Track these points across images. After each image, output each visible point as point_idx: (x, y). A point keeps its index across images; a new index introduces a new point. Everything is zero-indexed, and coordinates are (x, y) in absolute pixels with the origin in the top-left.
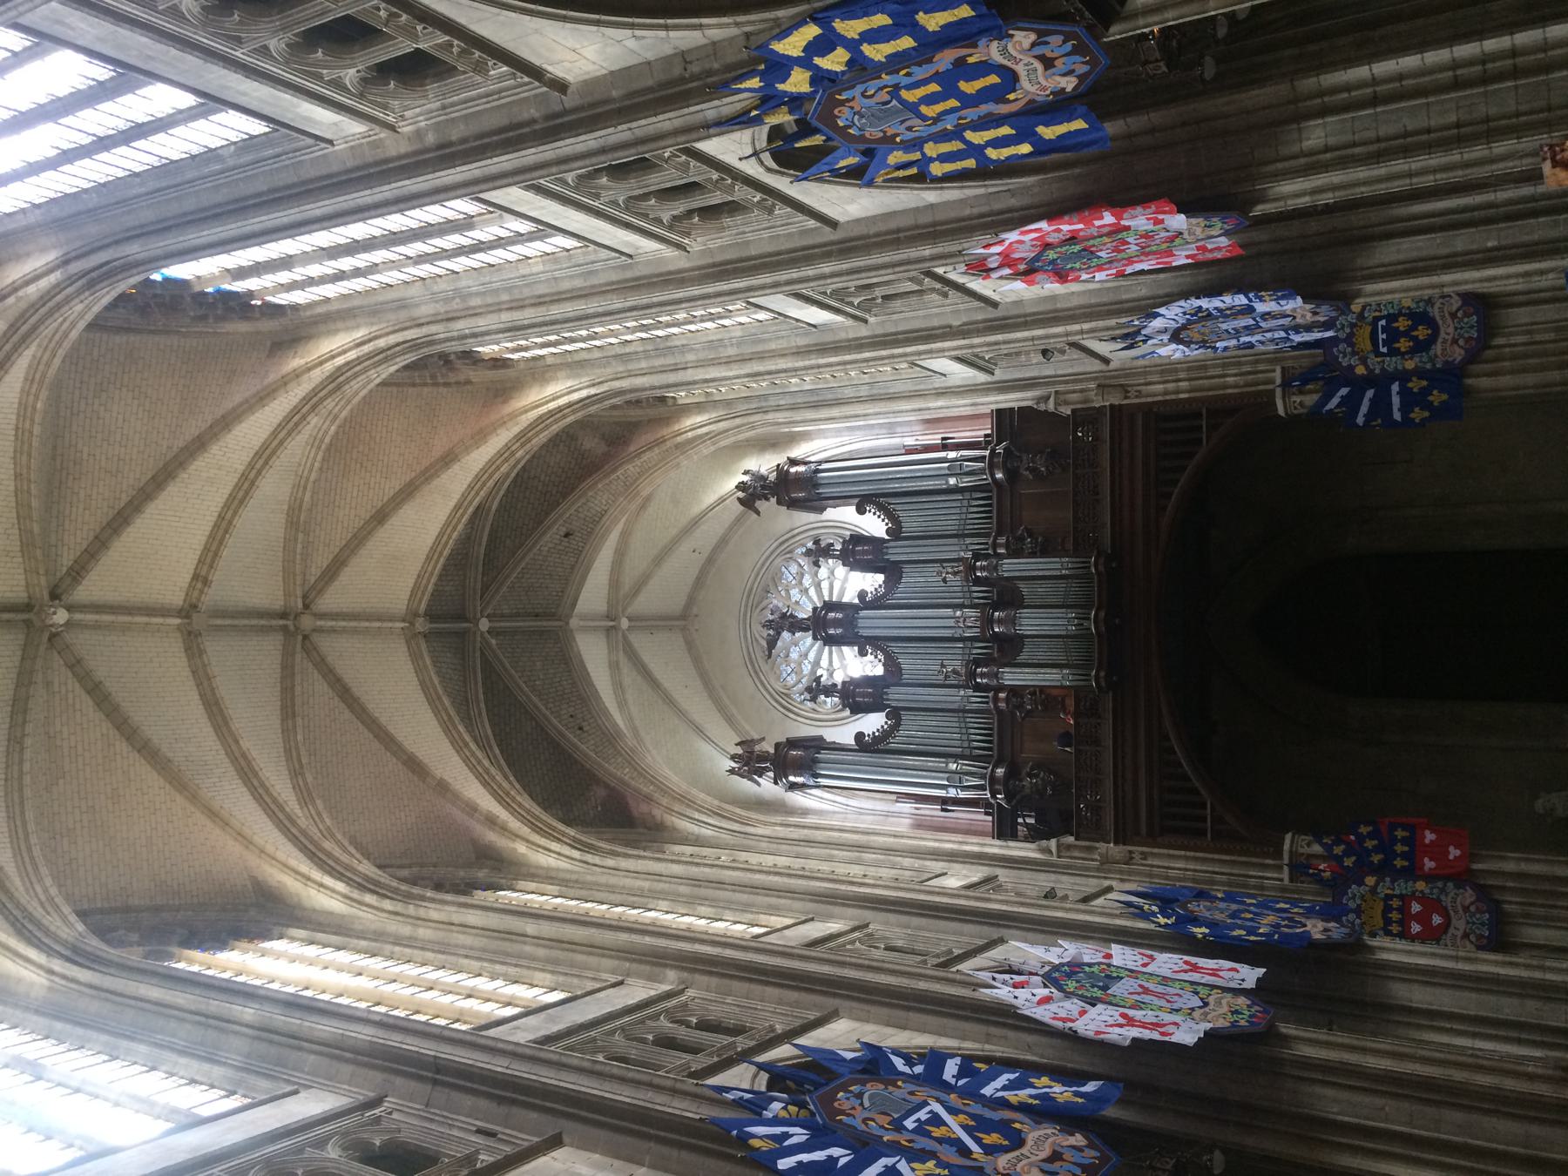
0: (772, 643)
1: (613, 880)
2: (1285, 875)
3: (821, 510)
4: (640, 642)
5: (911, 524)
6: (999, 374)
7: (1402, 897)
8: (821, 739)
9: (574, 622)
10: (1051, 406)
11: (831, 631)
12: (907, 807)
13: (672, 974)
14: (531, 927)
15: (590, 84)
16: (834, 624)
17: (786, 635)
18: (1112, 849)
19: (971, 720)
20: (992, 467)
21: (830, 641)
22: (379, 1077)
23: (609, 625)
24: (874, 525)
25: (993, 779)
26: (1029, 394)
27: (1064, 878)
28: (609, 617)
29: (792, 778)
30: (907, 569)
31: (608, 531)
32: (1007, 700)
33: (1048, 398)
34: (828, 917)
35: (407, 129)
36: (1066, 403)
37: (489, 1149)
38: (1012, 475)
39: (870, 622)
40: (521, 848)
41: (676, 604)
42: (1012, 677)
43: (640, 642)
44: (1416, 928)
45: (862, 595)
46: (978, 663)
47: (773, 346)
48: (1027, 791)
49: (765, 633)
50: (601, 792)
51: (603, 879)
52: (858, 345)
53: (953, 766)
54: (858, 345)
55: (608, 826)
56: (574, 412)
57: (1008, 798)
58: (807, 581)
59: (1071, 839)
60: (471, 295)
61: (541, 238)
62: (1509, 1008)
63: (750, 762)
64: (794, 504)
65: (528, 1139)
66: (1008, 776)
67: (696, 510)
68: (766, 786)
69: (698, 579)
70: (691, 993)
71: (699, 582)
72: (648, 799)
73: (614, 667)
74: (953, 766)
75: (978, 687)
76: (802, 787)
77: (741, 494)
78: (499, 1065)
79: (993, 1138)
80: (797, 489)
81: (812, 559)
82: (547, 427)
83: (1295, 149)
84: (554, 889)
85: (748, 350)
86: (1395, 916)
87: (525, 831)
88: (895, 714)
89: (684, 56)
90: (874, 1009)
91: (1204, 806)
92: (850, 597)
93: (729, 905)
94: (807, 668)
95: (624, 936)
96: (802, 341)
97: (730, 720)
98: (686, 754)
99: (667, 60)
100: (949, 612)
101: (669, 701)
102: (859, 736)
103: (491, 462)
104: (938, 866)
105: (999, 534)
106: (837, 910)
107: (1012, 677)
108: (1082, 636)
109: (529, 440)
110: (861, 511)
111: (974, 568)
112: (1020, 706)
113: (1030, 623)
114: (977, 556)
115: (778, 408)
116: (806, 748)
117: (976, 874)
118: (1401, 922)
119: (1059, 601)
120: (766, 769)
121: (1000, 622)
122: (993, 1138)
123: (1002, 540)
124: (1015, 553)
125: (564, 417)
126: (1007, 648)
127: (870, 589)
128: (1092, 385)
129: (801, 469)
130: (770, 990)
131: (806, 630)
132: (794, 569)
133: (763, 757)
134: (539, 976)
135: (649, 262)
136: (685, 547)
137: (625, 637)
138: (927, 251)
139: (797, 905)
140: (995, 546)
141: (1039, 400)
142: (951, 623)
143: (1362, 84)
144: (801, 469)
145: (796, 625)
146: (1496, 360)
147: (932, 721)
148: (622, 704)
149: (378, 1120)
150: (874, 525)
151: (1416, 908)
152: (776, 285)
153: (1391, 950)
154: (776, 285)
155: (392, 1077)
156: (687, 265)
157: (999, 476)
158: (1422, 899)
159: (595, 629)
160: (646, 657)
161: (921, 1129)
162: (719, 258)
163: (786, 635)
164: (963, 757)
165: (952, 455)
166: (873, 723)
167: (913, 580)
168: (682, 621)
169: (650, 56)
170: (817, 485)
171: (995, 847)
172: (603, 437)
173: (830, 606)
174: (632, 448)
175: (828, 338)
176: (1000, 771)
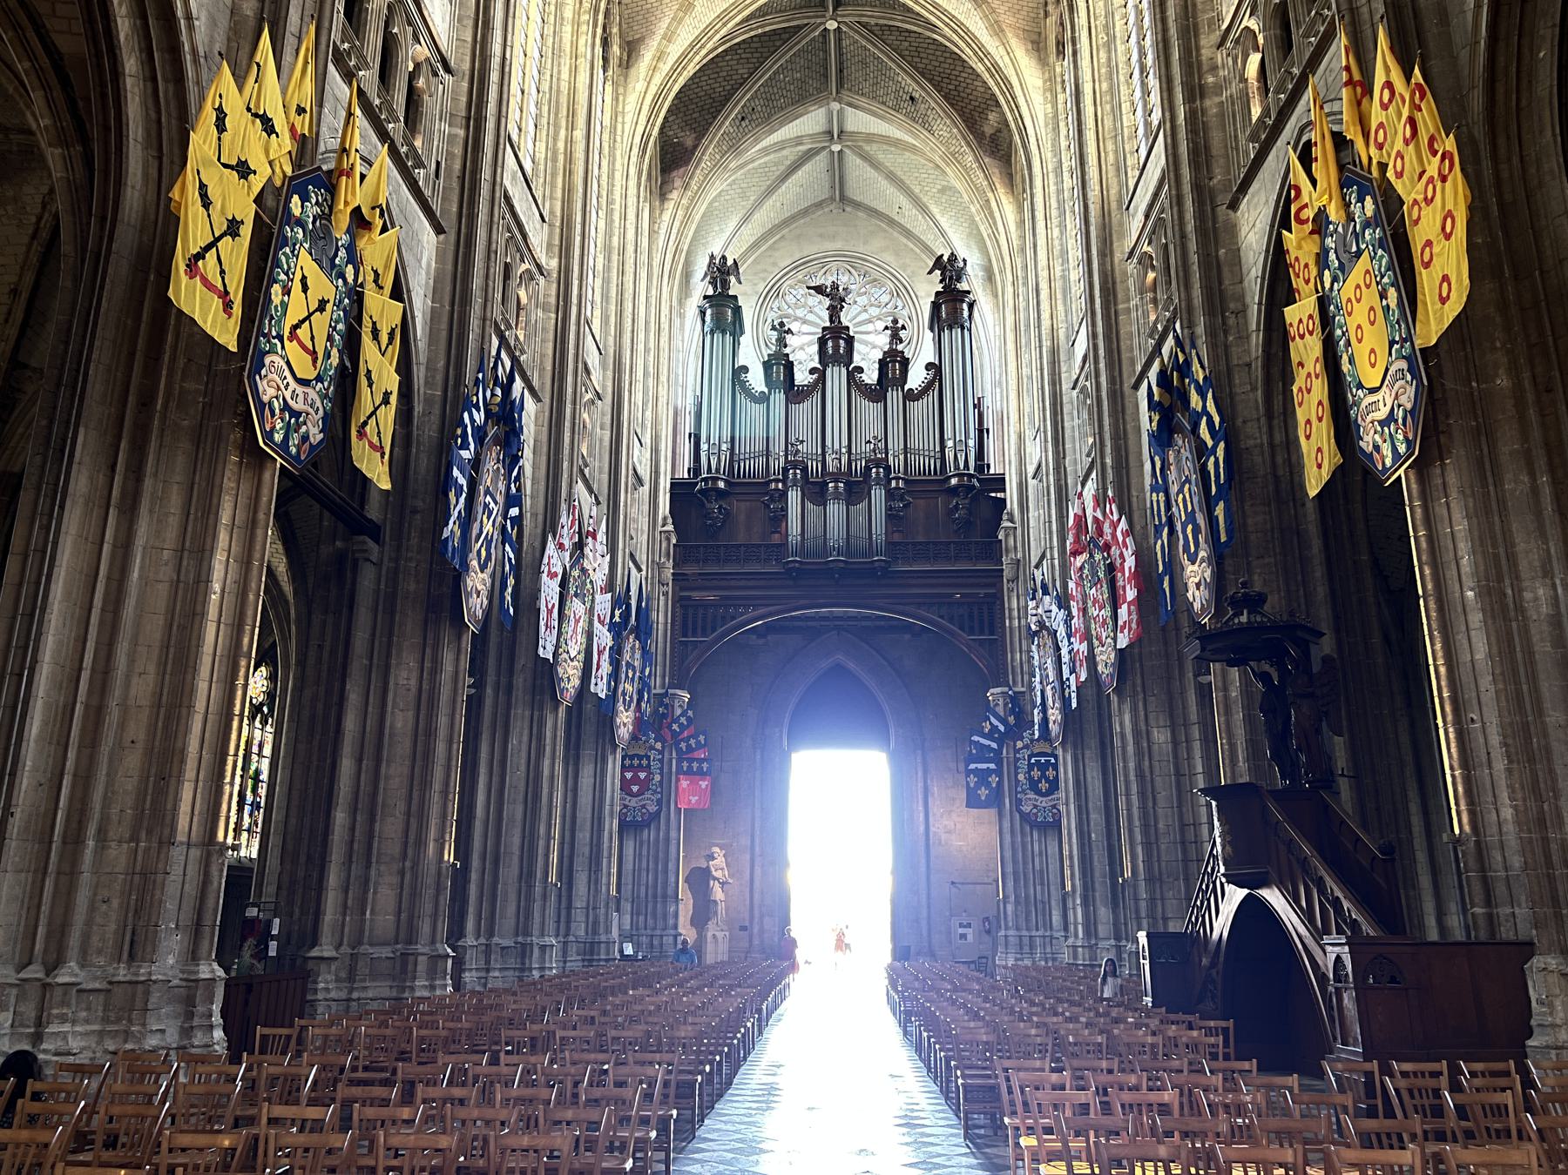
0: (819, 290)
1: (618, 175)
2: (658, 691)
3: (931, 329)
4: (820, 162)
5: (917, 408)
6: (1032, 483)
7: (649, 766)
8: (742, 333)
9: (835, 106)
10: (1006, 524)
11: (830, 344)
12: (690, 400)
13: (554, 263)
14: (579, 134)
15: (1232, 230)
16: (836, 342)
17: (827, 302)
19: (762, 461)
20: (960, 476)
21: (822, 342)
22: (466, 66)
23: (835, 133)
25: (716, 479)
26: (1015, 506)
27: (645, 537)
28: (841, 132)
29: (709, 312)
30: (880, 405)
31: (916, 137)
32: (777, 489)
33: (1012, 521)
34: (604, 366)
35: (1219, 57)
36: (1007, 536)
37: (427, 176)
38: (954, 491)
39: (836, 378)
40: (640, 86)
41: (853, 192)
42: (794, 497)
43: (820, 162)
44: (629, 775)
45: (860, 370)
46: (805, 470)
47: (1060, 307)
48: (708, 505)
49: (829, 283)
50: (689, 142)
51: (618, 166)
52: (1055, 381)
53: (724, 447)
54: (1055, 381)
55: (662, 149)
56: (1015, 120)
57: (701, 491)
58: (874, 311)
59: (674, 541)
60: (1109, 52)
61: (1146, 135)
62: (583, 836)
63: (722, 272)
64: (936, 307)
65: (436, 207)
66: (718, 490)
67: (935, 210)
68: (701, 288)
69: (876, 211)
70: (542, 281)
71: (874, 213)
72: (686, 187)
73: (798, 140)
74: (724, 447)
75: (785, 470)
76: (704, 321)
77: (945, 258)
78: (486, 174)
79: (484, 553)
80: (951, 307)
81: (890, 324)
82: (1003, 93)
83: (1152, 722)
84: (607, 122)
85: (1058, 284)
86: (636, 762)
87: (653, 90)
88: (763, 399)
89: (1242, 312)
90: (545, 429)
91: (704, 634)
92: (857, 360)
93: (606, 281)
94: (800, 313)
95: (579, 219)
96: (1062, 333)
97: (755, 246)
98: (730, 204)
99: (1241, 298)
100: (845, 442)
101: (770, 191)
102: (745, 369)
103: (974, 38)
104: (647, 440)
105: (906, 481)
106: (610, 373)
107: (794, 497)
108: (825, 550)
109: (992, 76)
110: (929, 366)
111: (877, 467)
112: (772, 500)
113: (835, 510)
114: (888, 469)
115: (1016, 295)
116: (734, 323)
117: (645, 472)
118: (631, 766)
119: (852, 532)
120: (715, 288)
121: (836, 487)
122: (484, 553)
123: (901, 484)
124: (891, 494)
125: (1011, 110)
126: (816, 491)
127: (864, 377)
128: (1020, 555)
129: (966, 314)
130: (550, 345)
131: (831, 321)
132: (885, 298)
133: (725, 285)
134: (541, 146)
135: (1121, 224)
136: (903, 200)
137: (824, 148)
138: (1108, 461)
139: (611, 340)
140: (897, 479)
141: (1011, 515)
142: (837, 446)
143: (1191, 766)
144: (966, 314)
145: (834, 312)
146: (1023, 834)
148: (766, 151)
149: (435, 74)
150: (917, 377)
151: (642, 775)
152: (1095, 336)
153: (614, 765)
154: (1095, 336)
155: (467, 78)
156: (1116, 260)
157: (954, 481)
158: (648, 779)
159: (830, 121)
160: (807, 167)
161: (486, 506)
162: (1119, 287)
163: (827, 302)
164: (732, 454)
165: (971, 443)
166: (756, 379)
167: (869, 411)
168: (840, 196)
169: (1246, 283)
170: (951, 328)
171: (665, 484)
172: (999, 131)
173: (850, 341)
174: (987, 160)
175: (1062, 358)
176: (721, 484)
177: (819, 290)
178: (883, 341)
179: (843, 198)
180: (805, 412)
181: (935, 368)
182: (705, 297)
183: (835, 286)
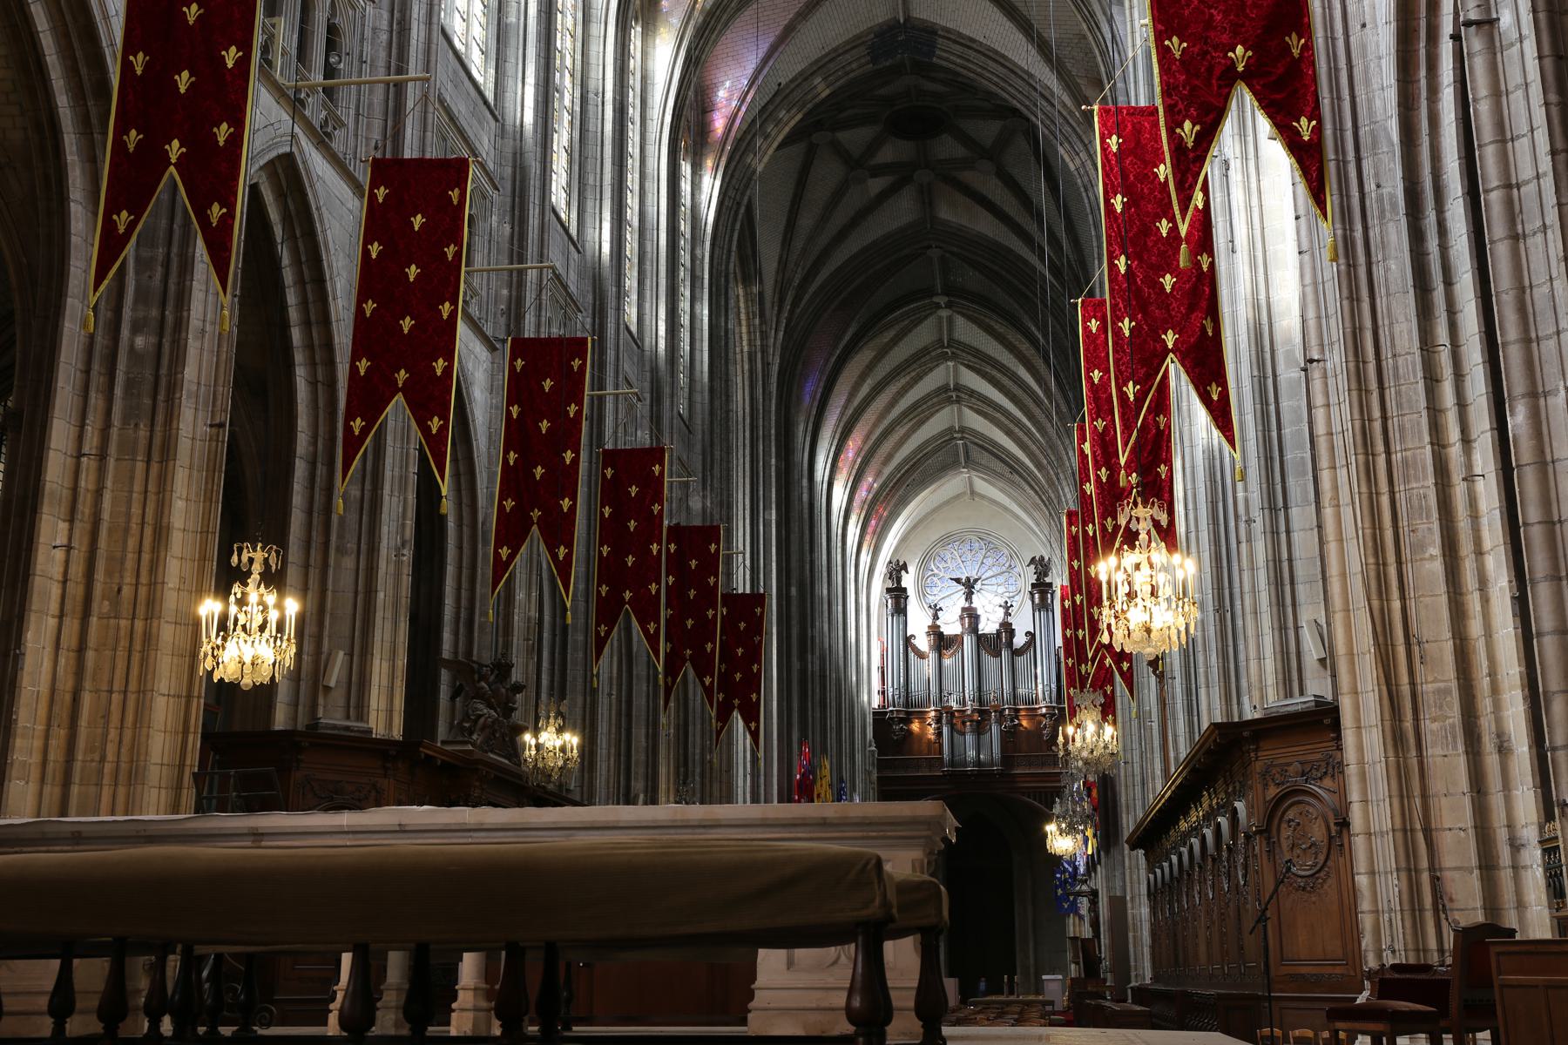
0: (958, 581)
5: (1020, 660)
16: (971, 616)
21: (962, 618)
24: (1020, 640)
58: (995, 570)
63: (897, 570)
110: (1028, 633)
132: (1003, 560)
133: (899, 580)
150: (1020, 640)
166: (923, 643)
167: (989, 662)
177: (958, 581)
179: (973, 492)
182: (889, 590)
183: (968, 579)
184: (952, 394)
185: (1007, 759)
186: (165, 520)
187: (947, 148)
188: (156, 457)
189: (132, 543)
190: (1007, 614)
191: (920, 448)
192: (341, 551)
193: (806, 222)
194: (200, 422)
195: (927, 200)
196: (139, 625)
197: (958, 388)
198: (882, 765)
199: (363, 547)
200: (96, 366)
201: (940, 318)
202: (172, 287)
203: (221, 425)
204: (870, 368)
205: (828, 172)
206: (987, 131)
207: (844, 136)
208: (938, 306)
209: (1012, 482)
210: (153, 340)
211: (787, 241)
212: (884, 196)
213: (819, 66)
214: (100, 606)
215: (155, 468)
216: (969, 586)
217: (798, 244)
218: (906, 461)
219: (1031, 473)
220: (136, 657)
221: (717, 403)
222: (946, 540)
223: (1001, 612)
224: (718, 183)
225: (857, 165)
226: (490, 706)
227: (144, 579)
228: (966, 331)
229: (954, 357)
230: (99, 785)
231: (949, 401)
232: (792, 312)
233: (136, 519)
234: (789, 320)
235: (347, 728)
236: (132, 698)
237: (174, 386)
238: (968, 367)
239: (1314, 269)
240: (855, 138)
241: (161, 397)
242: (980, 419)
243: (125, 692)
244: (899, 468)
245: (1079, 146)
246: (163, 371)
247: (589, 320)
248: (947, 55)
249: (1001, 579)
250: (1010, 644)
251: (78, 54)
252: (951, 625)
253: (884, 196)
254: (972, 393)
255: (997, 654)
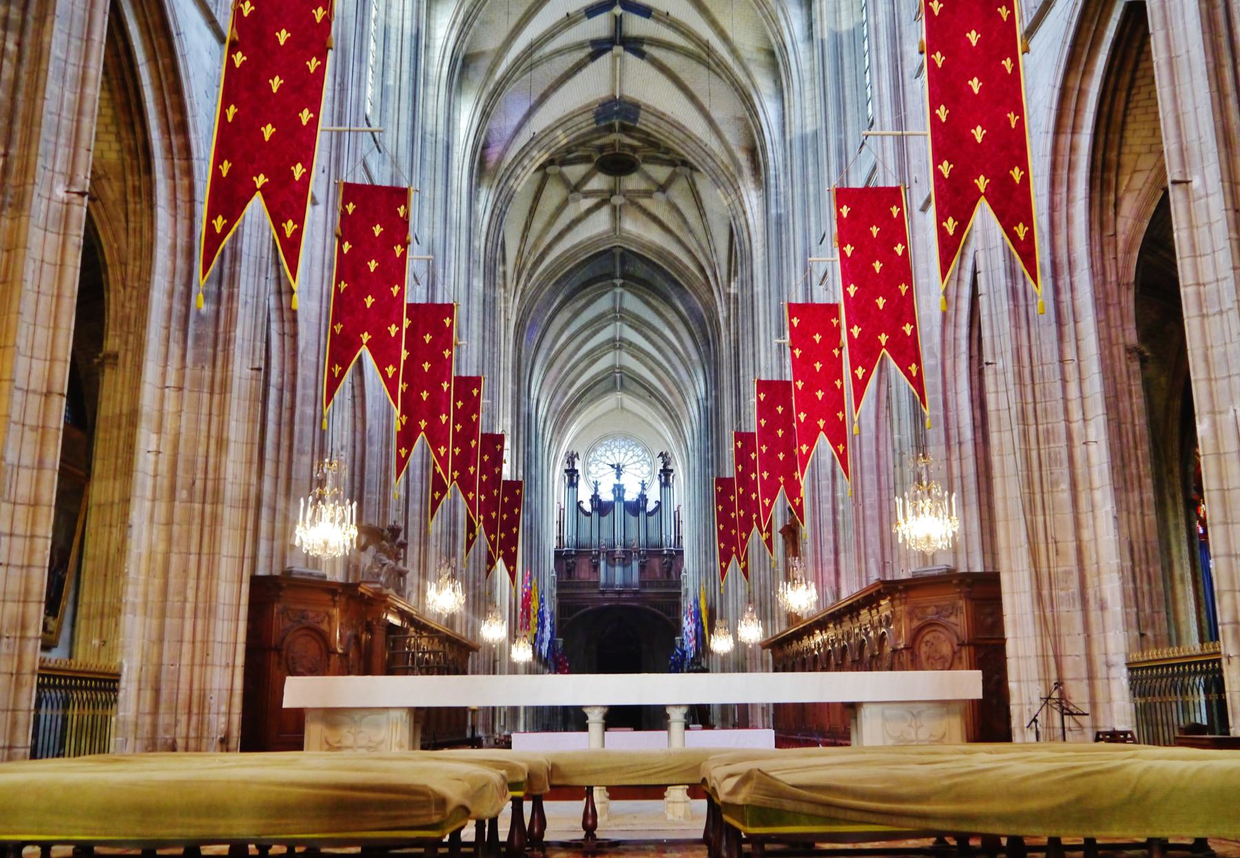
0: (612, 466)
5: (651, 519)
9: (619, 395)
16: (618, 490)
18: (555, 593)
21: (614, 491)
24: (651, 506)
58: (635, 459)
63: (571, 458)
71: (636, 415)
107: (602, 564)
113: (618, 570)
147: (588, 528)
150: (651, 506)
166: (587, 507)
167: (632, 520)
178: (639, 489)
179: (622, 408)
180: (605, 520)
181: (659, 503)
184: (616, 344)
185: (643, 584)
186: (225, 435)
187: (633, 182)
188: (217, 389)
189: (201, 450)
190: (643, 488)
191: (592, 378)
192: (301, 452)
193: (537, 225)
194: (244, 366)
195: (616, 213)
196: (208, 508)
197: (621, 340)
198: (560, 585)
199: (316, 450)
200: (174, 325)
201: (615, 294)
202: (226, 271)
203: (259, 369)
204: (568, 324)
205: (554, 194)
206: (661, 173)
207: (567, 170)
208: (615, 286)
209: (650, 403)
210: (213, 307)
211: (524, 237)
212: (590, 211)
213: (561, 123)
214: (182, 494)
215: (216, 398)
216: (618, 469)
217: (531, 239)
218: (583, 385)
219: (665, 398)
220: (206, 530)
221: (487, 347)
222: (605, 437)
223: (640, 487)
224: (491, 198)
225: (575, 189)
226: (389, 558)
227: (211, 475)
228: (632, 303)
229: (622, 319)
230: (183, 617)
231: (615, 348)
232: (525, 286)
233: (204, 434)
234: (523, 291)
235: (310, 574)
236: (204, 558)
237: (228, 342)
238: (630, 326)
239: (990, 305)
240: (575, 172)
241: (220, 348)
242: (634, 360)
243: (200, 554)
244: (578, 391)
245: (731, 190)
246: (221, 329)
247: (424, 291)
248: (645, 122)
249: (638, 465)
250: (644, 508)
251: (168, 102)
252: (607, 496)
253: (590, 211)
254: (631, 344)
255: (636, 514)
